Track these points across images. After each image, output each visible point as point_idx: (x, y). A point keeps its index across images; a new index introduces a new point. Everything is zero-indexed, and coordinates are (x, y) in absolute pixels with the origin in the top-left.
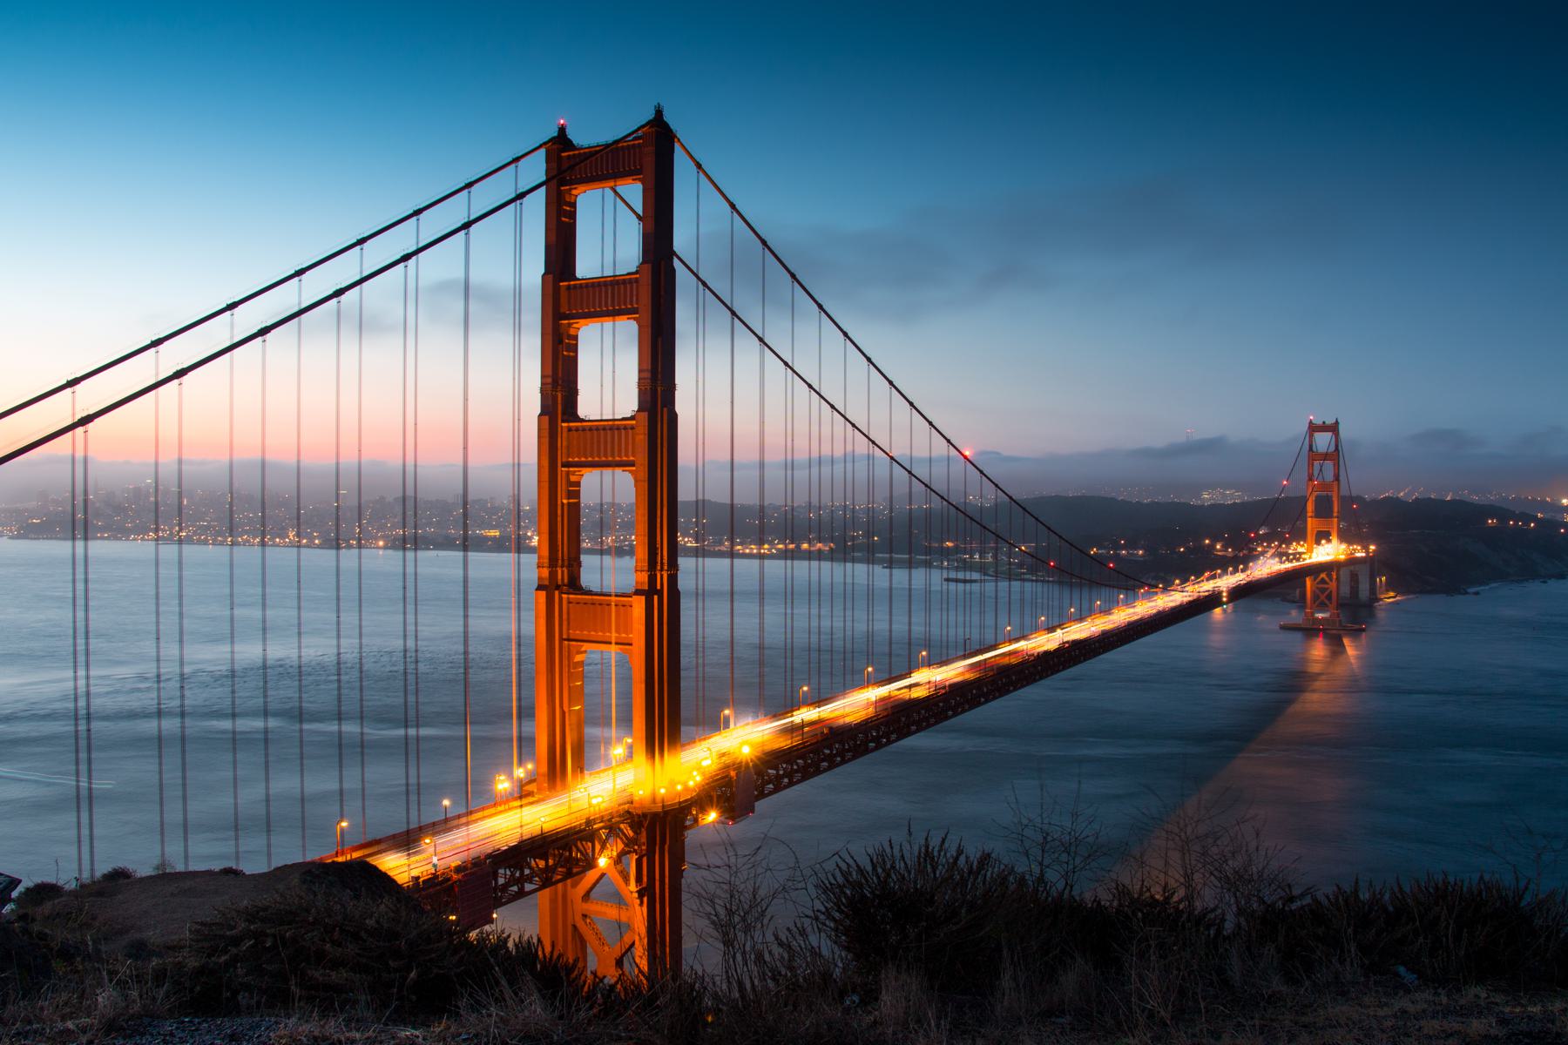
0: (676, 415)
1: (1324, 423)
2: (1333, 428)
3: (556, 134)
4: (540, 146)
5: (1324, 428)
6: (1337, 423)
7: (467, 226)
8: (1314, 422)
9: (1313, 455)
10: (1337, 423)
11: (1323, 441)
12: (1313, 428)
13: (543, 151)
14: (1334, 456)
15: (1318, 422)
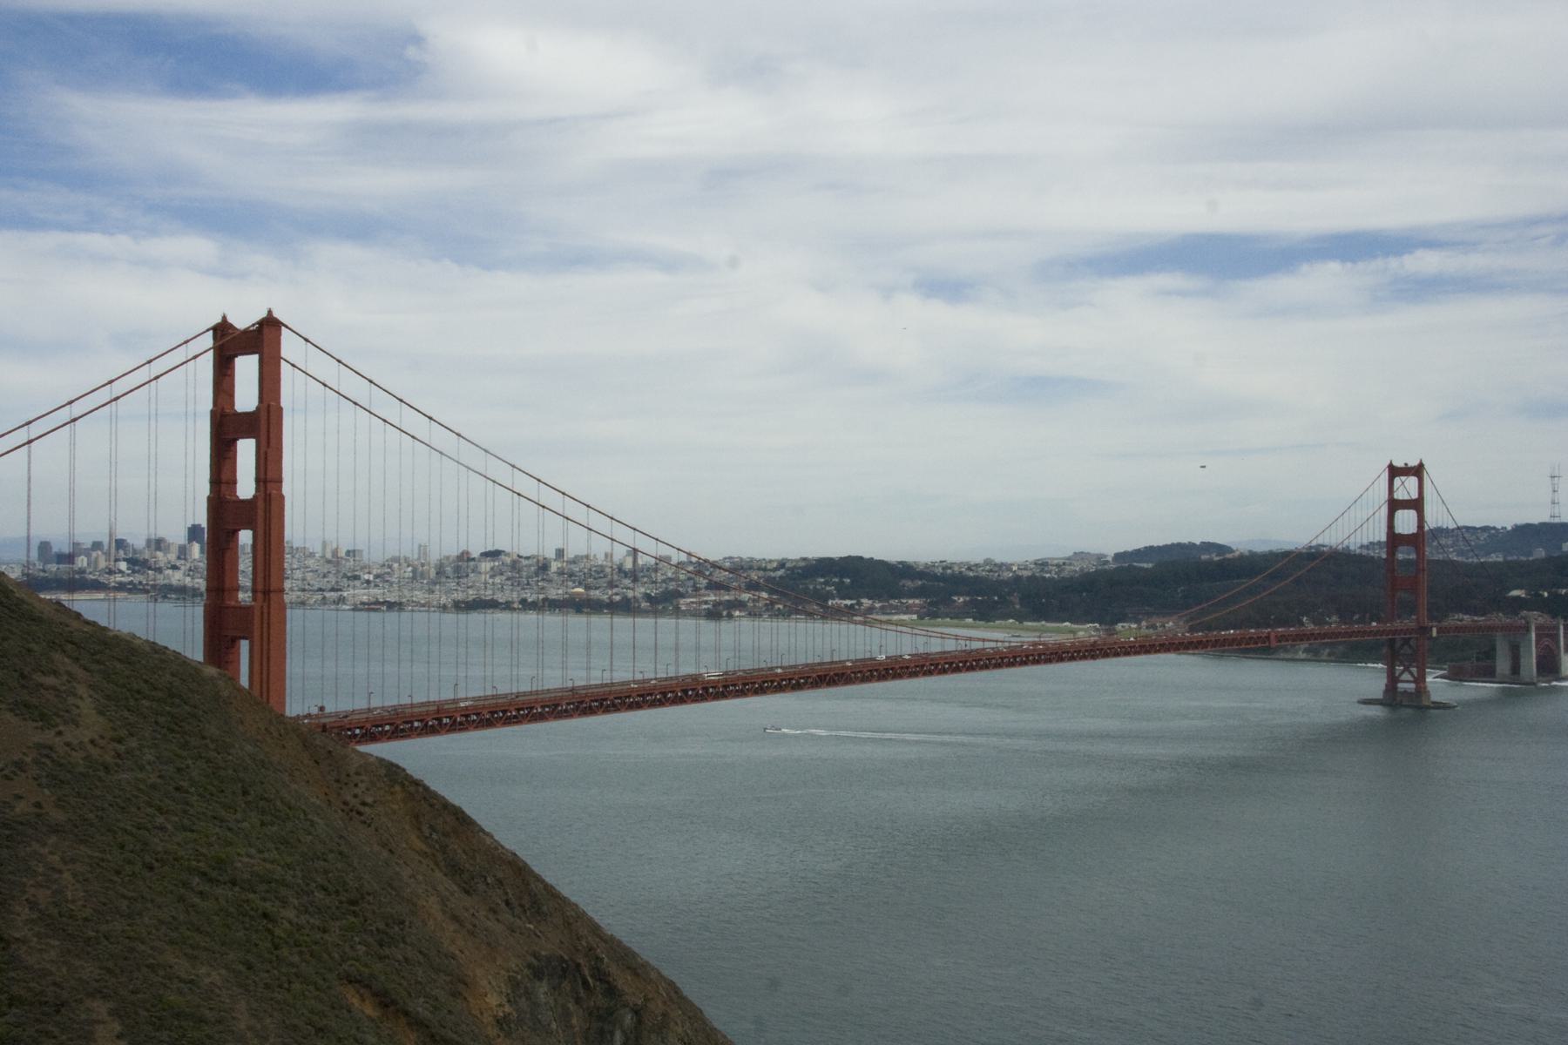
0: (282, 498)
1: (1406, 464)
2: (1418, 471)
3: (220, 321)
4: (208, 330)
5: (1406, 471)
6: (1421, 466)
7: (117, 398)
8: (1395, 464)
9: (1394, 505)
10: (1421, 466)
11: (1407, 488)
12: (1394, 472)
13: (211, 332)
14: (1417, 505)
15: (1403, 465)
